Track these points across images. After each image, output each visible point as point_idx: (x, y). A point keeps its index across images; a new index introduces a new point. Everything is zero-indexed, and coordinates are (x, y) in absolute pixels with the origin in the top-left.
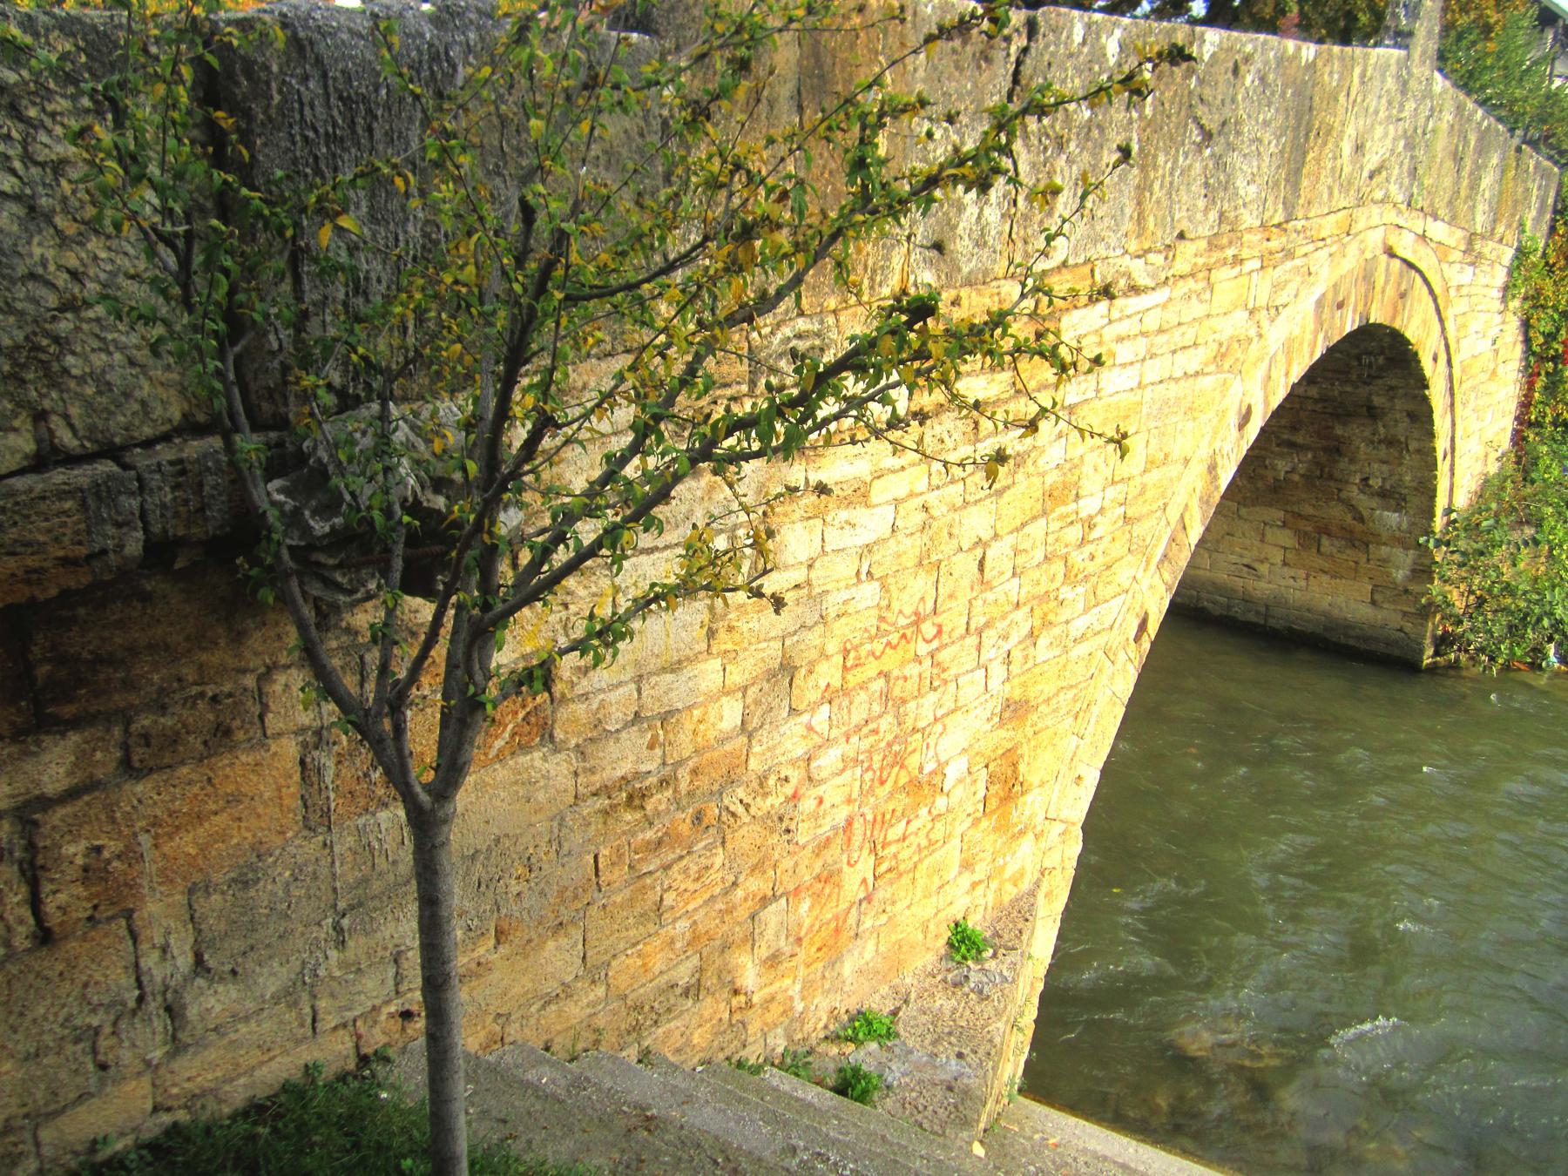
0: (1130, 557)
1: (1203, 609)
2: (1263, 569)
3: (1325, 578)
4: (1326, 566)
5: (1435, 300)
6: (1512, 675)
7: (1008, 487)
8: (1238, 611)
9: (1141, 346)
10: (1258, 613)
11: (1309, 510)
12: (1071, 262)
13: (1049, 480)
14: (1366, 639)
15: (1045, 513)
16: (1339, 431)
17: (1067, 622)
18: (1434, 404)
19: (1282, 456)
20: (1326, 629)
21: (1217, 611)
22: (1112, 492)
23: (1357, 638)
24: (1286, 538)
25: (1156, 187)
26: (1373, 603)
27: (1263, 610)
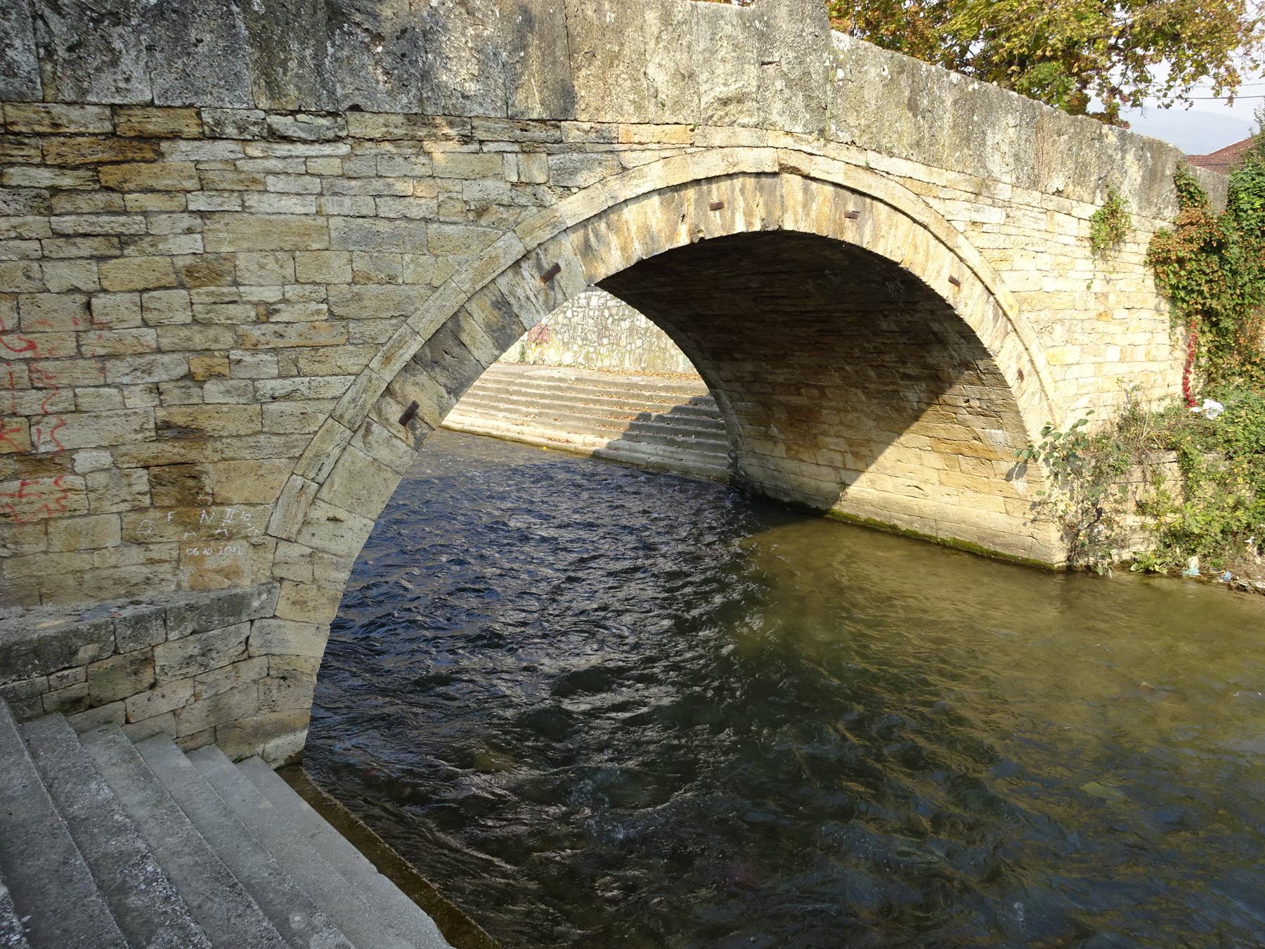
0: (351, 348)
1: (894, 527)
2: (927, 488)
3: (969, 493)
4: (968, 483)
5: (925, 227)
6: (1151, 582)
7: (116, 257)
8: (917, 527)
9: (316, 185)
10: (931, 528)
11: (943, 434)
12: (157, 102)
13: (180, 262)
14: (1007, 546)
15: (182, 286)
16: (930, 360)
17: (253, 380)
18: (971, 321)
19: (907, 387)
20: (980, 538)
21: (903, 527)
22: (291, 291)
23: (1002, 545)
24: (934, 460)
25: (293, 64)
26: (1007, 513)
27: (933, 524)
